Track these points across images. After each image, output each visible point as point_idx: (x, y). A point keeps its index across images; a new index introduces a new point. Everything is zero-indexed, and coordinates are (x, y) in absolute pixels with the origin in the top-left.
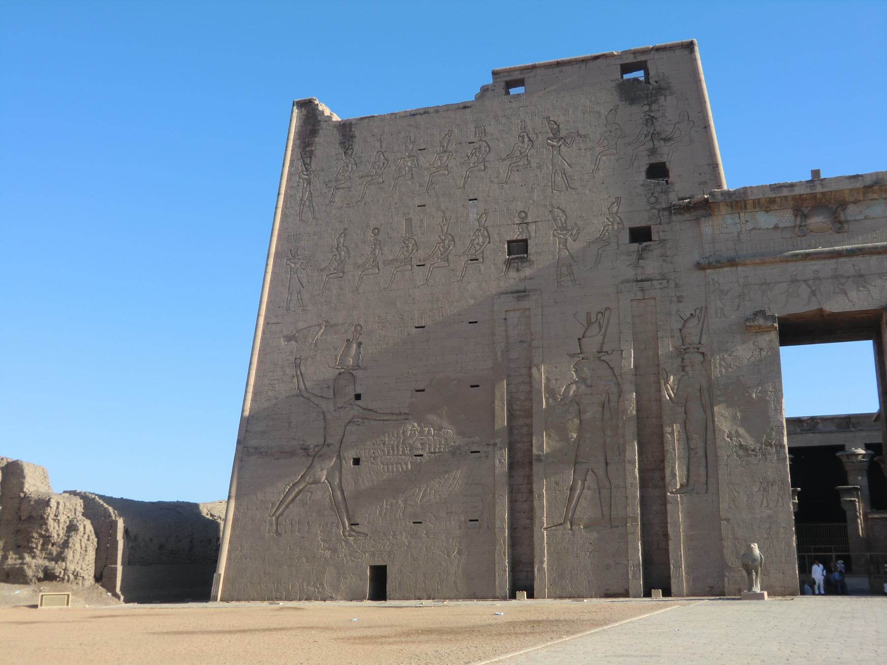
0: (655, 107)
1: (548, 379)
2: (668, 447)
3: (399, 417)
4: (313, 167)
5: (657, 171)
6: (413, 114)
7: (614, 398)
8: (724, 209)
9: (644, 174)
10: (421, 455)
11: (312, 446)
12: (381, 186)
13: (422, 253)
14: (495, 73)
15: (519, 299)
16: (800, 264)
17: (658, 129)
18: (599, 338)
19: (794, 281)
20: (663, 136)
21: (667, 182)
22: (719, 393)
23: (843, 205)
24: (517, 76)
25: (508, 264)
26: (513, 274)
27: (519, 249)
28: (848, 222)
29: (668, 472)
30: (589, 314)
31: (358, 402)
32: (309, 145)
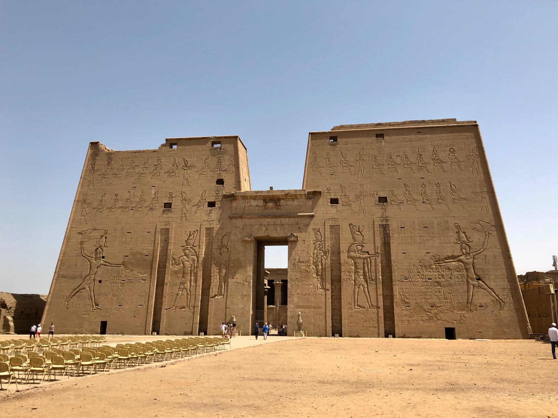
1: (173, 254)
2: (212, 281)
5: (220, 182)
6: (135, 152)
8: (240, 198)
13: (133, 205)
14: (166, 140)
15: (166, 225)
16: (263, 220)
18: (193, 241)
19: (261, 225)
20: (223, 169)
23: (279, 200)
24: (174, 142)
25: (164, 212)
26: (165, 215)
27: (168, 206)
28: (280, 206)
29: (211, 290)
30: (190, 232)
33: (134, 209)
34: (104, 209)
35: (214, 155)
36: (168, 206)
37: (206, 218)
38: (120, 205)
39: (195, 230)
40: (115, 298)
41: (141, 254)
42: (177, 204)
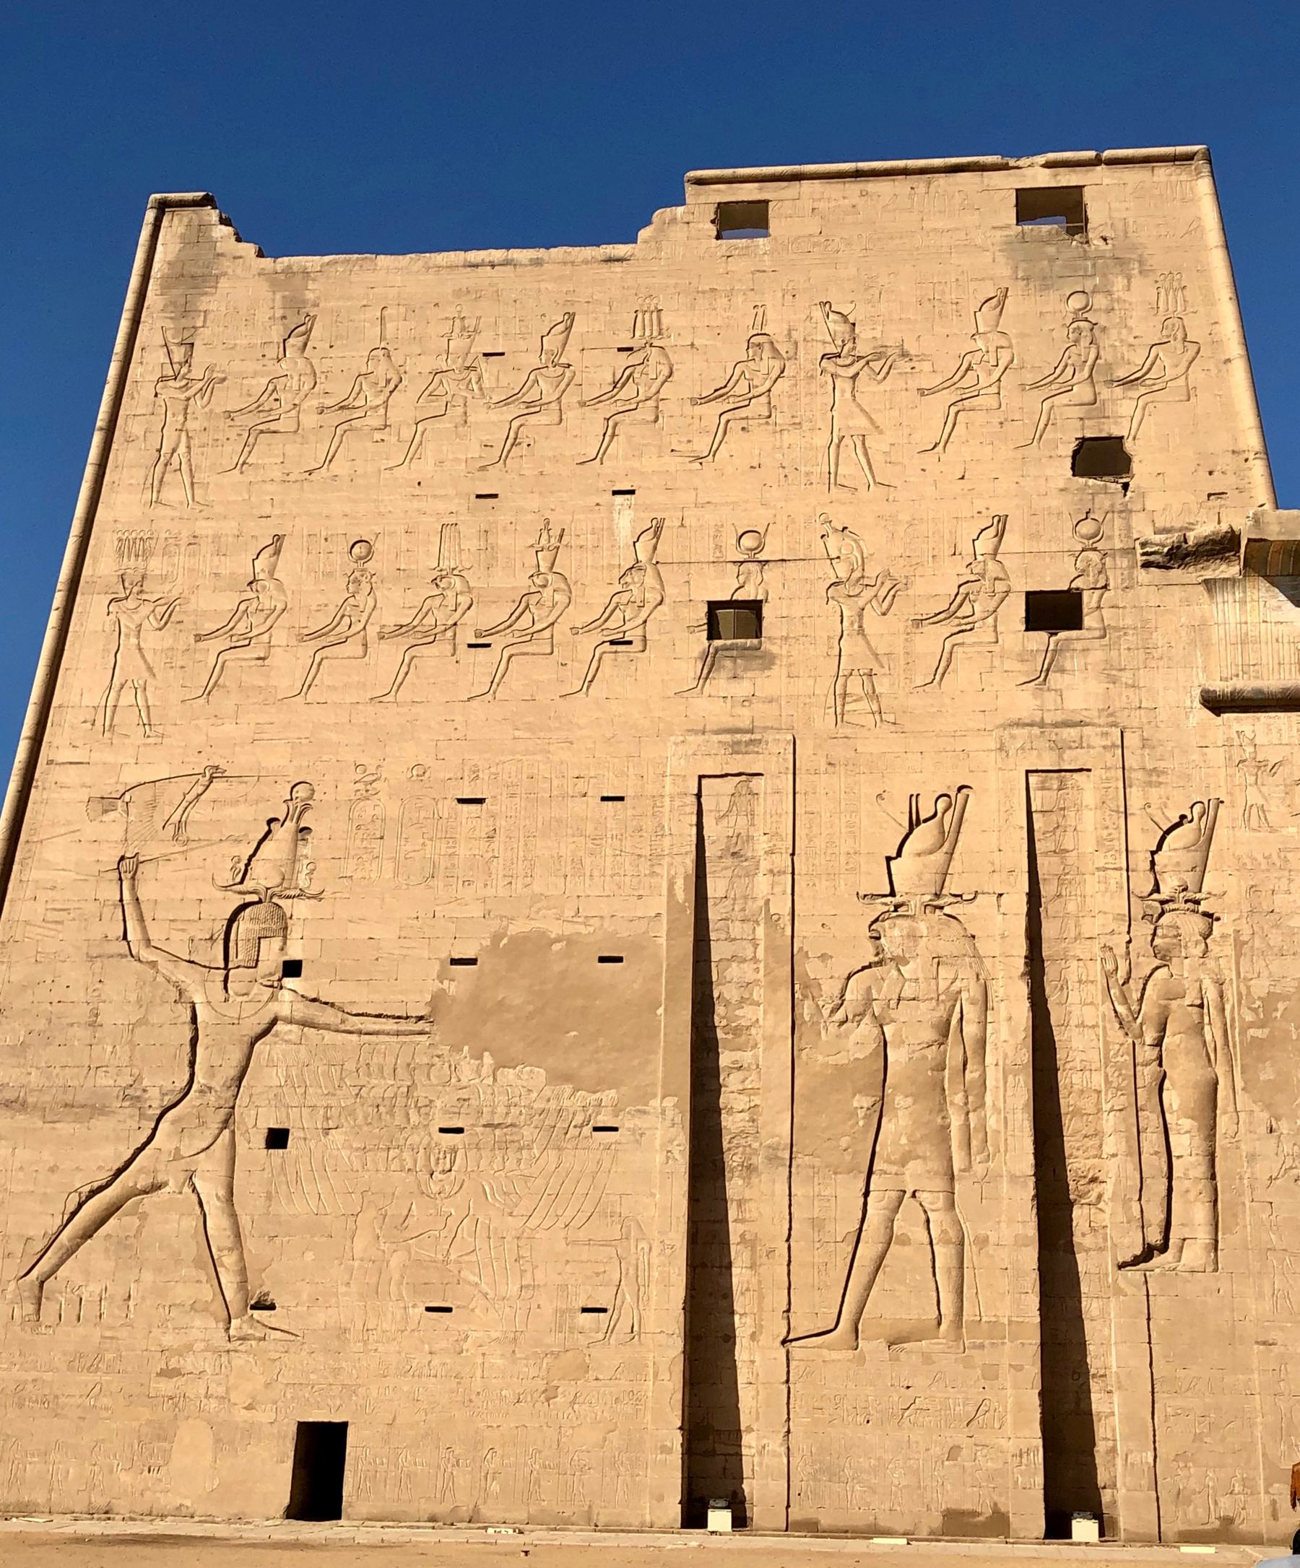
0: (1100, 301)
3: (404, 1026)
4: (197, 373)
5: (1101, 458)
7: (971, 1013)
9: (1069, 462)
10: (459, 1131)
11: (154, 1093)
12: (377, 436)
15: (735, 748)
17: (1106, 355)
18: (939, 857)
20: (1121, 373)
21: (1126, 487)
22: (1249, 1017)
24: (748, 192)
26: (720, 684)
27: (736, 621)
31: (289, 982)
32: (185, 313)
33: (497, 641)
34: (280, 637)
35: (1046, 283)
36: (736, 621)
37: (1025, 703)
38: (390, 620)
39: (948, 782)
40: (396, 1261)
41: (570, 941)
42: (798, 611)
